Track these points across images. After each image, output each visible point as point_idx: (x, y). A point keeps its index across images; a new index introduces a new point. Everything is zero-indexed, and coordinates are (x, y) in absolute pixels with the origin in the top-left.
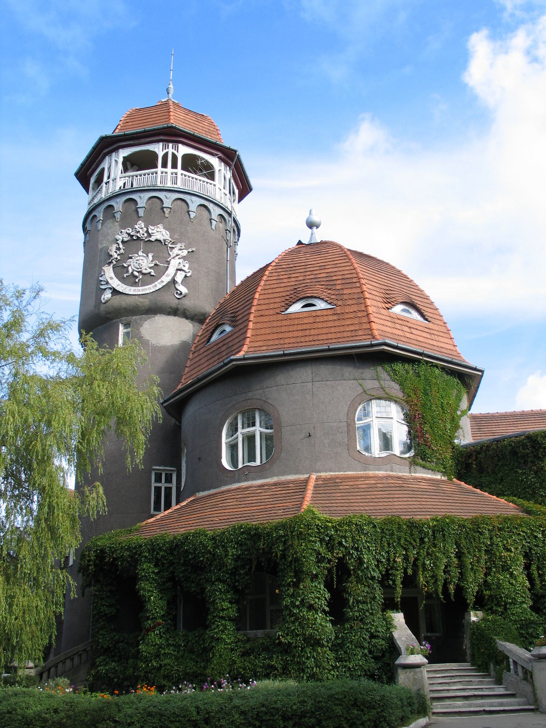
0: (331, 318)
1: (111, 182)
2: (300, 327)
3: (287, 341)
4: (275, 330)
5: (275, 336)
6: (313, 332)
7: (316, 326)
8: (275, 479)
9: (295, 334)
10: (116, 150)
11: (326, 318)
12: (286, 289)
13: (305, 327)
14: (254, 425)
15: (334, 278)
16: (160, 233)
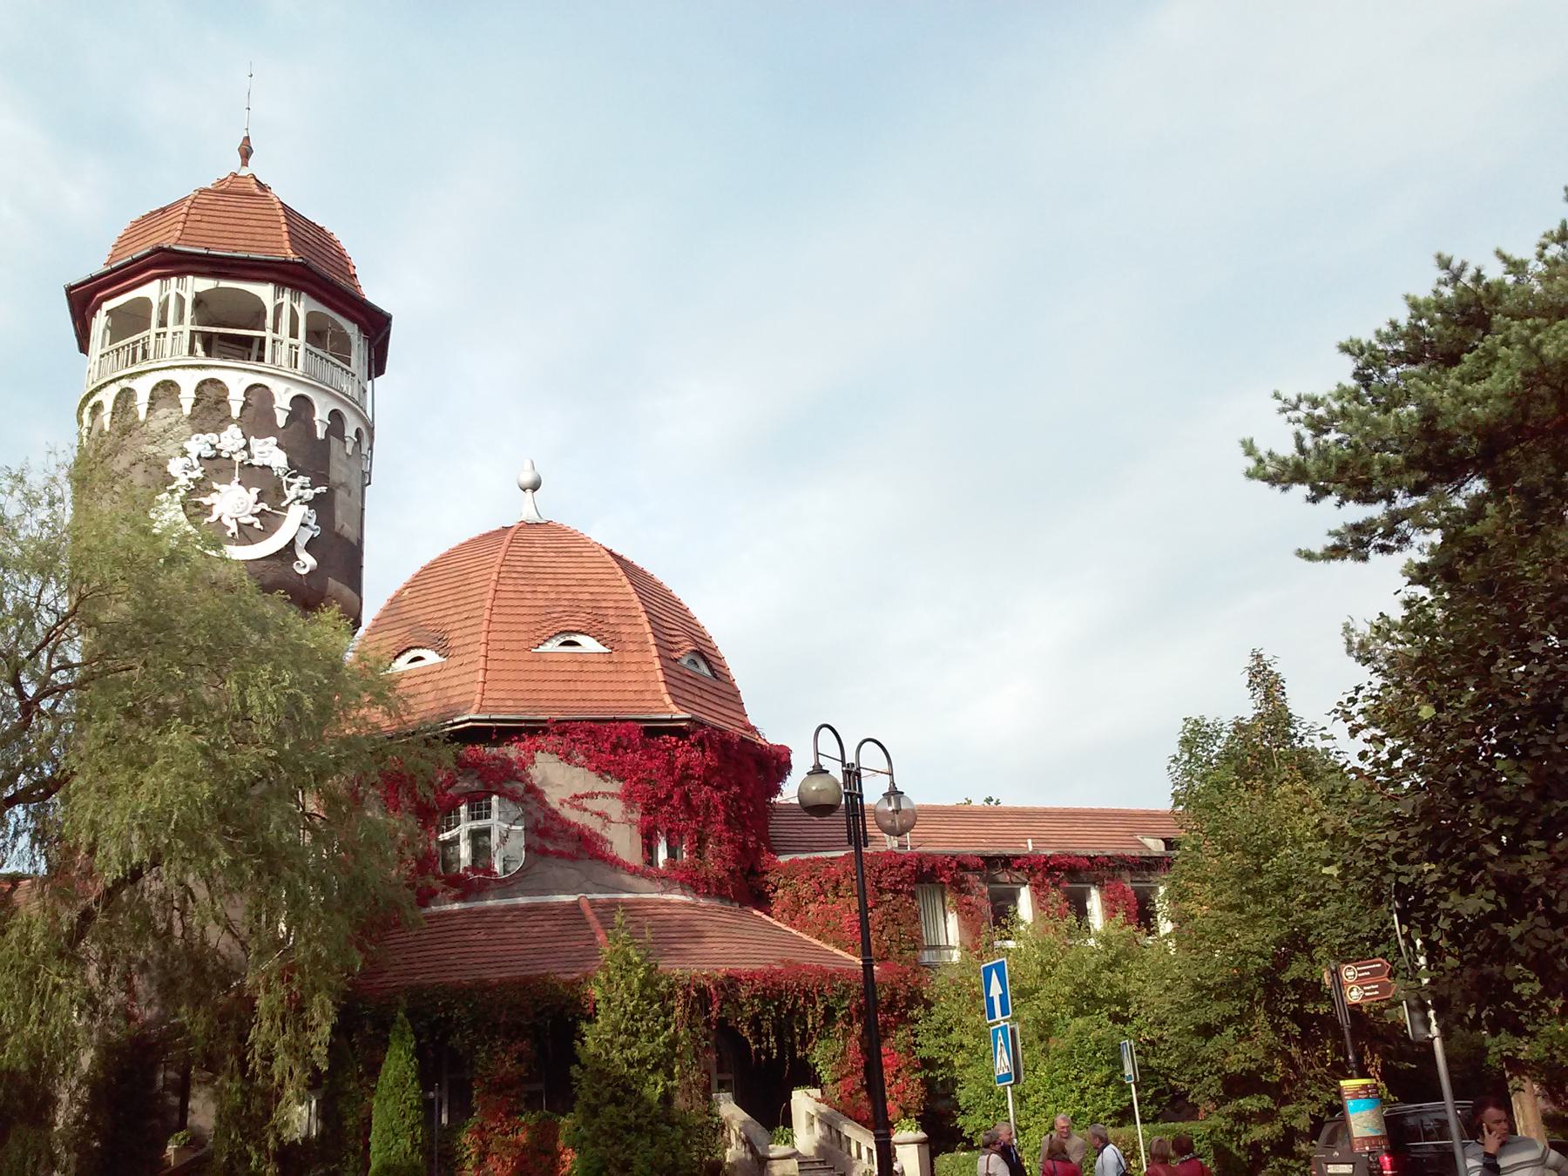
0: (603, 668)
1: (169, 335)
2: (561, 677)
3: (544, 696)
4: (524, 676)
5: (524, 686)
6: (580, 686)
7: (583, 676)
8: (522, 900)
9: (555, 686)
10: (181, 274)
11: (597, 667)
12: (533, 611)
13: (567, 676)
14: (488, 816)
15: (604, 604)
16: (270, 454)
